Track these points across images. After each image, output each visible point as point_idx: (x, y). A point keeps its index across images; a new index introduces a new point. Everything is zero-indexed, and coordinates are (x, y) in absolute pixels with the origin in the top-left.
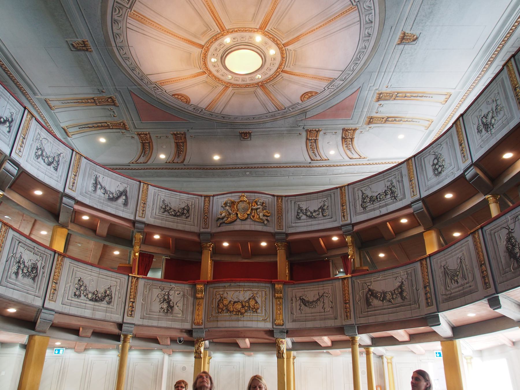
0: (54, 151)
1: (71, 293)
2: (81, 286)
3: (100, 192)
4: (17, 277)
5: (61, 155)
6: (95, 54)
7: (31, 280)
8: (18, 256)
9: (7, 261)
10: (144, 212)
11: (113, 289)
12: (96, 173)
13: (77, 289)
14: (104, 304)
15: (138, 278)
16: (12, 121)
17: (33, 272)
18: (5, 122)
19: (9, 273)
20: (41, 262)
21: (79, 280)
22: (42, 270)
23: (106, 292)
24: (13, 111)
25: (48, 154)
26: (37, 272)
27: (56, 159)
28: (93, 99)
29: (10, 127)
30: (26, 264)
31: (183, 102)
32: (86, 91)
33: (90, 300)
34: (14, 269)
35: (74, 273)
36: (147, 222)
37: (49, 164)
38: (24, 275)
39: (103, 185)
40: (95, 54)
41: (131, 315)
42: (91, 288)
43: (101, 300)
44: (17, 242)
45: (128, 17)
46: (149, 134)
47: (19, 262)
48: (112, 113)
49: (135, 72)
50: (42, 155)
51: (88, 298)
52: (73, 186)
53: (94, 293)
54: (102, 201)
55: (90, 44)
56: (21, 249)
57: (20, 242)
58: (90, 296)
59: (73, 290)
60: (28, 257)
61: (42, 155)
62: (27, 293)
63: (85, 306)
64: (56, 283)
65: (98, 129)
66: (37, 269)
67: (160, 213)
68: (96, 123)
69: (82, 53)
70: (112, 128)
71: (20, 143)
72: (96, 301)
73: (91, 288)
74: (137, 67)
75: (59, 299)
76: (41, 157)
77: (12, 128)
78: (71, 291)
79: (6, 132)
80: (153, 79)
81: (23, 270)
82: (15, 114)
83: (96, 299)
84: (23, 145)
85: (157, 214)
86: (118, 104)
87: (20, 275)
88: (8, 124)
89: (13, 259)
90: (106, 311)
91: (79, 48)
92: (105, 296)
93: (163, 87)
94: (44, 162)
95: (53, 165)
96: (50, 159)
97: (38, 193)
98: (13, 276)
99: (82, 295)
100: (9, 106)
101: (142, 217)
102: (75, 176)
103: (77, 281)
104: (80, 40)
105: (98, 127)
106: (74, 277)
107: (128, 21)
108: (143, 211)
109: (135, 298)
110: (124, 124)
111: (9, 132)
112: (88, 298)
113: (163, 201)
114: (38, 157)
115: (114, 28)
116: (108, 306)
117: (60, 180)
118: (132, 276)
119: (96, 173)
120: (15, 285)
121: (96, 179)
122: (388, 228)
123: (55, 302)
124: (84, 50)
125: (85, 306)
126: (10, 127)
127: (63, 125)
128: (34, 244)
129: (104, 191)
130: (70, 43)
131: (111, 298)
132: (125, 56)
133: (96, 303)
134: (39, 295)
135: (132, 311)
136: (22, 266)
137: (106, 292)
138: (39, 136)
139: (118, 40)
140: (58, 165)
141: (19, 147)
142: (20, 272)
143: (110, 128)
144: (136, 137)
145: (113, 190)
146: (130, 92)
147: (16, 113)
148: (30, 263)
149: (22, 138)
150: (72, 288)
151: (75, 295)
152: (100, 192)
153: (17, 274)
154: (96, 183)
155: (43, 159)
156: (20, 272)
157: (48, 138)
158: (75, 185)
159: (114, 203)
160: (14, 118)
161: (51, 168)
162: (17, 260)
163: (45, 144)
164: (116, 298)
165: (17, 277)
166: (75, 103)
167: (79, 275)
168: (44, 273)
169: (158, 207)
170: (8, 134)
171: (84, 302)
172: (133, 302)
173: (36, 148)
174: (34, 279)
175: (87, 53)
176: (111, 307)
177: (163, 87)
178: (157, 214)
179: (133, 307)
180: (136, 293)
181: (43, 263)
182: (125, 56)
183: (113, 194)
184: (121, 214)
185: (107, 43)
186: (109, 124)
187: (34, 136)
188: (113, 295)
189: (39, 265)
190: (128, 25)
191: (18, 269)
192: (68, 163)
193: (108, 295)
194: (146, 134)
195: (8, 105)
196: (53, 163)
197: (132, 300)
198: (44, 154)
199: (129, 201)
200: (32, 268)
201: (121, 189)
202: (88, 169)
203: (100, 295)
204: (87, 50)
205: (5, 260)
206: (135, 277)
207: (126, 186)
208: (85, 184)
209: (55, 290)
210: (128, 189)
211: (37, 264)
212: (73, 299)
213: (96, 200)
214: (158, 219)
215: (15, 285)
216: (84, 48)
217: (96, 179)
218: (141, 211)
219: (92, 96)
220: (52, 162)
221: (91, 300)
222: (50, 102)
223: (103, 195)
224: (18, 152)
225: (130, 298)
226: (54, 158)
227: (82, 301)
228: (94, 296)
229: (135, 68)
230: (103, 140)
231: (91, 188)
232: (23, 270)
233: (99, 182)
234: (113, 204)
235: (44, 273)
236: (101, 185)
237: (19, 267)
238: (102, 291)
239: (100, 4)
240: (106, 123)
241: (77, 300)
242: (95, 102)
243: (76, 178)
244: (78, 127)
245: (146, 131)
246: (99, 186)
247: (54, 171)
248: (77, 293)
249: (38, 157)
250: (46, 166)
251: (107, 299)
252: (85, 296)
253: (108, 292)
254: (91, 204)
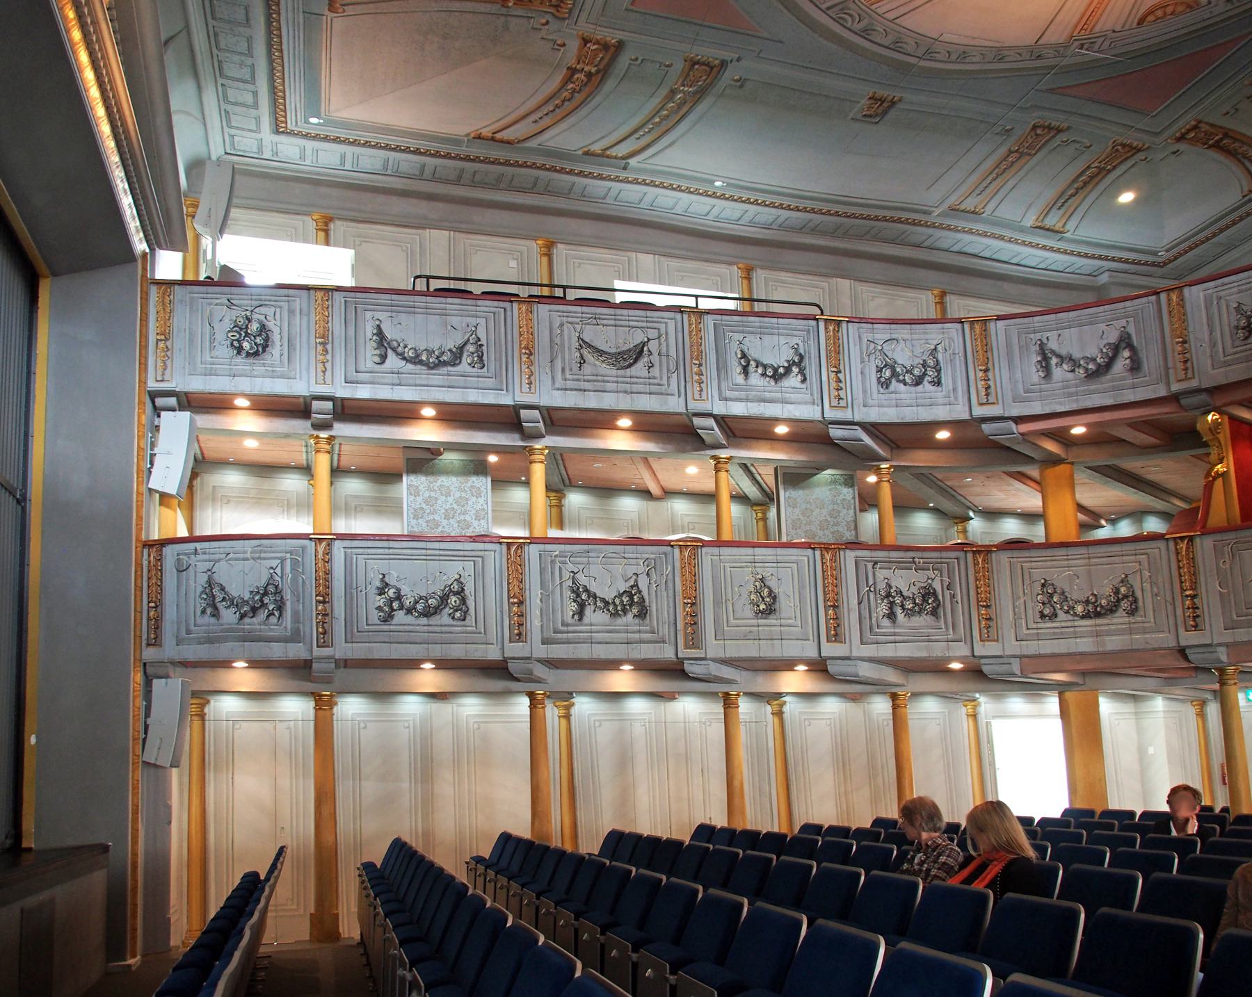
0: (918, 351)
1: (1033, 613)
2: (1051, 596)
3: (1060, 373)
4: (894, 622)
5: (939, 347)
6: (908, 96)
7: (929, 619)
8: (882, 586)
9: (859, 604)
10: (1189, 364)
11: (1135, 582)
12: (1038, 336)
13: (1043, 604)
14: (1120, 618)
15: (1191, 539)
16: (802, 357)
17: (928, 602)
18: (788, 370)
19: (874, 620)
20: (938, 579)
21: (1043, 585)
22: (947, 593)
23: (1117, 592)
24: (796, 340)
25: (908, 365)
26: (936, 599)
27: (931, 362)
28: (1010, 152)
29: (802, 372)
30: (905, 593)
31: (1181, 13)
32: (986, 153)
33: (1083, 617)
34: (883, 608)
35: (1027, 576)
36: (1205, 385)
37: (918, 381)
38: (909, 613)
39: (1064, 352)
40: (908, 96)
41: (1196, 626)
42: (1077, 592)
43: (1112, 610)
44: (870, 566)
45: (873, 7)
46: (1200, 122)
47: (888, 595)
48: (1077, 146)
49: (1007, 59)
50: (894, 374)
51: (1075, 614)
52: (987, 395)
53: (1087, 602)
54: (1073, 390)
55: (882, 92)
56: (881, 574)
57: (876, 563)
58: (1079, 609)
59: (1034, 608)
60: (905, 581)
61: (894, 374)
62: (929, 641)
63: (1075, 632)
64: (987, 607)
65: (1090, 186)
66: (935, 594)
67: (1238, 343)
68: (1075, 180)
69: (892, 114)
70: (1114, 168)
71: (833, 384)
72: (1098, 615)
73: (1077, 592)
74: (1000, 49)
75: (1009, 634)
76: (893, 381)
77: (807, 372)
78: (1030, 612)
79: (799, 385)
80: (1056, 36)
81: (902, 606)
82: (801, 344)
83: (1095, 611)
84: (842, 385)
85: (1230, 350)
86: (1065, 125)
87: (900, 616)
88: (795, 369)
89: (872, 595)
90: (1131, 632)
91: (880, 111)
92: (1118, 601)
93: (1097, 29)
94: (905, 384)
95: (927, 378)
96: (916, 372)
97: (943, 435)
98: (886, 622)
99: (1060, 613)
100: (783, 340)
101: (1186, 379)
102: (986, 371)
103: (1038, 589)
104: (864, 102)
105: (1085, 184)
106: (1027, 582)
107: (880, 11)
108: (1186, 362)
109: (1194, 585)
110: (1124, 146)
111: (804, 381)
112: (1075, 614)
113: (1238, 309)
114: (885, 384)
115: (878, 40)
116: (1132, 619)
117: (956, 398)
118: (1175, 539)
119: (1038, 336)
120: (895, 634)
121: (1042, 347)
122: (127, 802)
123: (997, 641)
124: (890, 107)
125: (1075, 632)
126: (802, 372)
127: (1030, 221)
128: (911, 554)
129: (1071, 363)
130: (859, 116)
131: (1136, 601)
132: (954, 57)
133: (1099, 621)
134: (957, 637)
135: (1195, 618)
136: (898, 600)
137: (1117, 592)
138: (872, 346)
139: (910, 48)
140: (939, 371)
141: (834, 393)
142: (899, 611)
143: (1109, 171)
144: (1182, 146)
145: (1092, 351)
146: (1051, 91)
147: (804, 341)
148: (914, 590)
149: (833, 375)
150: (1029, 605)
151: (1043, 616)
152: (1059, 373)
153: (891, 616)
154: (1045, 358)
155: (899, 381)
156: (899, 611)
157: (894, 336)
158: (992, 390)
159: (1104, 379)
160: (802, 351)
161: (927, 386)
162: (883, 593)
163: (893, 350)
164: (1148, 595)
165: (894, 622)
166: (994, 180)
167: (1039, 575)
168: (953, 596)
169: (1227, 329)
170: (804, 386)
171: (1069, 624)
172: (1193, 597)
173: (874, 370)
174: (934, 613)
175: (900, 106)
176: (1139, 619)
177: (1097, 29)
178: (1230, 350)
179: (1195, 608)
180: (1194, 574)
181: (946, 579)
182: (954, 57)
183: (1094, 360)
184: (1130, 396)
185: (903, 68)
186: (1096, 164)
187: (861, 353)
188: (1138, 594)
189: (937, 585)
190: (891, 16)
191: (891, 608)
192: (962, 354)
193: (1125, 597)
194: (1195, 127)
195: (782, 338)
196: (928, 373)
197: (1188, 593)
198: (898, 370)
199: (1143, 355)
200: (923, 596)
201: (1113, 337)
202: (1015, 340)
203: (1104, 602)
204: (893, 103)
205: (856, 602)
206: (1182, 538)
207: (1123, 322)
208: (1019, 375)
209: (990, 619)
210: (1131, 330)
211: (930, 585)
212: (1040, 625)
213: (1060, 393)
214: (1238, 361)
215: (895, 634)
216: (885, 105)
217: (1042, 347)
218: (1180, 366)
219: (1003, 150)
220: (925, 374)
221: (1086, 616)
222: (962, 207)
223: (1070, 375)
224: (835, 403)
225: (1183, 590)
226: (924, 365)
227: (1063, 624)
228: (1090, 608)
229: (1000, 54)
230: (1127, 197)
231: (1035, 376)
232: (902, 606)
233: (1053, 352)
234: (1105, 381)
235: (953, 596)
236: (1058, 356)
237: (892, 604)
238: (1108, 590)
239: (816, 36)
240: (1089, 167)
241: (1049, 625)
242: (1022, 153)
243: (990, 375)
244: (1054, 210)
245: (1189, 120)
246: (1054, 361)
247: (934, 388)
248: (1047, 611)
249: (885, 384)
250: (913, 389)
251: (1124, 604)
252: (1067, 612)
253: (1123, 590)
254: (1047, 410)
